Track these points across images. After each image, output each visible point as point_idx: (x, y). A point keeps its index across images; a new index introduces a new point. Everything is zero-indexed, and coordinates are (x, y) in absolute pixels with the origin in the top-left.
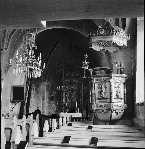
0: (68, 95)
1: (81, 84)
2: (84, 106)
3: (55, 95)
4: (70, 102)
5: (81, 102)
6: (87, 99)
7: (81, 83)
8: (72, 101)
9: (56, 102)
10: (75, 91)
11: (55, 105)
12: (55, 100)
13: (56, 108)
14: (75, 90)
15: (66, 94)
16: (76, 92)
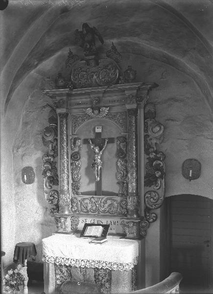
0: (83, 162)
1: (134, 112)
2: (148, 210)
3: (37, 160)
4: (92, 187)
5: (138, 194)
6: (161, 177)
7: (134, 106)
8: (99, 185)
9: (40, 187)
10: (110, 145)
11: (40, 199)
12: (36, 179)
13: (41, 212)
14: (111, 141)
15: (75, 157)
16: (113, 147)
